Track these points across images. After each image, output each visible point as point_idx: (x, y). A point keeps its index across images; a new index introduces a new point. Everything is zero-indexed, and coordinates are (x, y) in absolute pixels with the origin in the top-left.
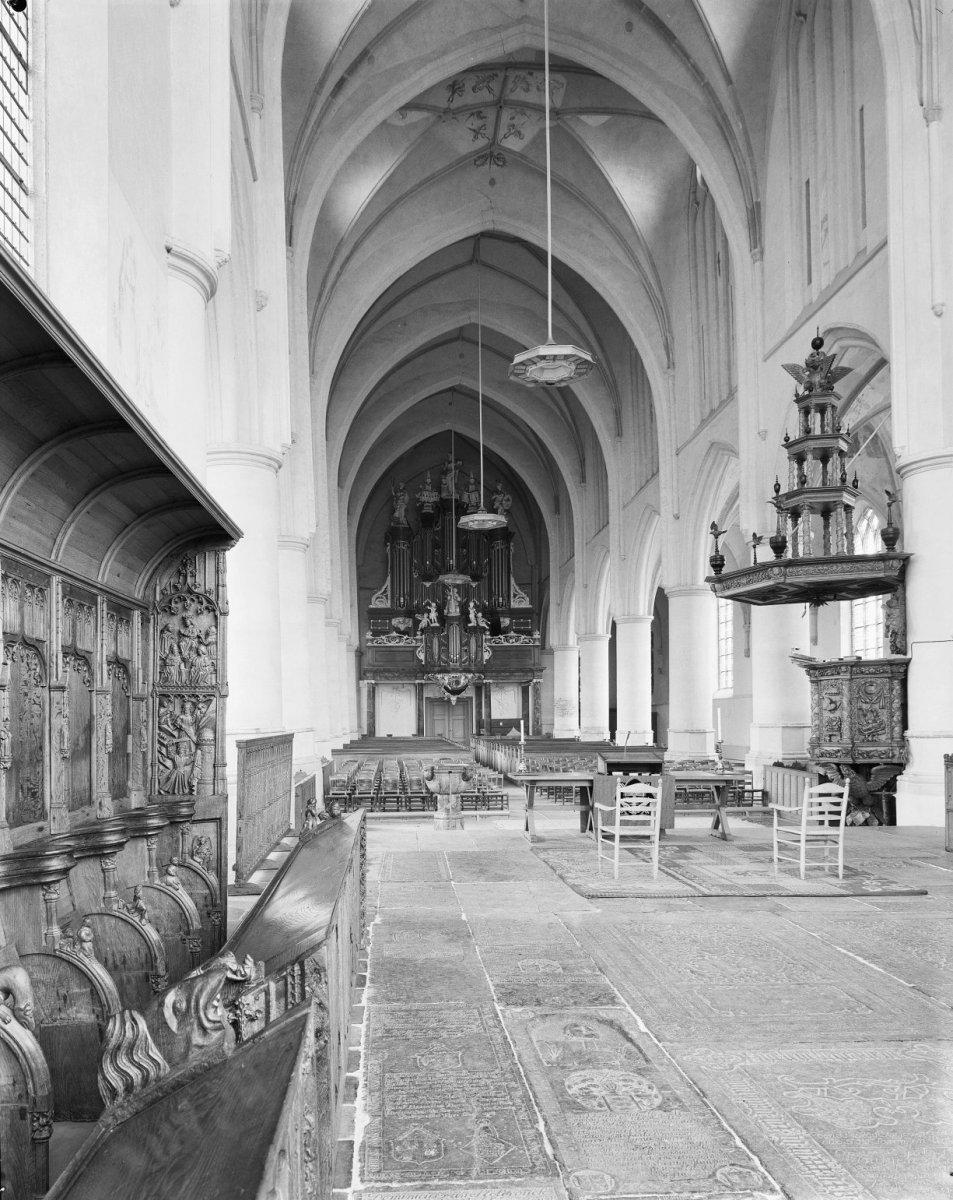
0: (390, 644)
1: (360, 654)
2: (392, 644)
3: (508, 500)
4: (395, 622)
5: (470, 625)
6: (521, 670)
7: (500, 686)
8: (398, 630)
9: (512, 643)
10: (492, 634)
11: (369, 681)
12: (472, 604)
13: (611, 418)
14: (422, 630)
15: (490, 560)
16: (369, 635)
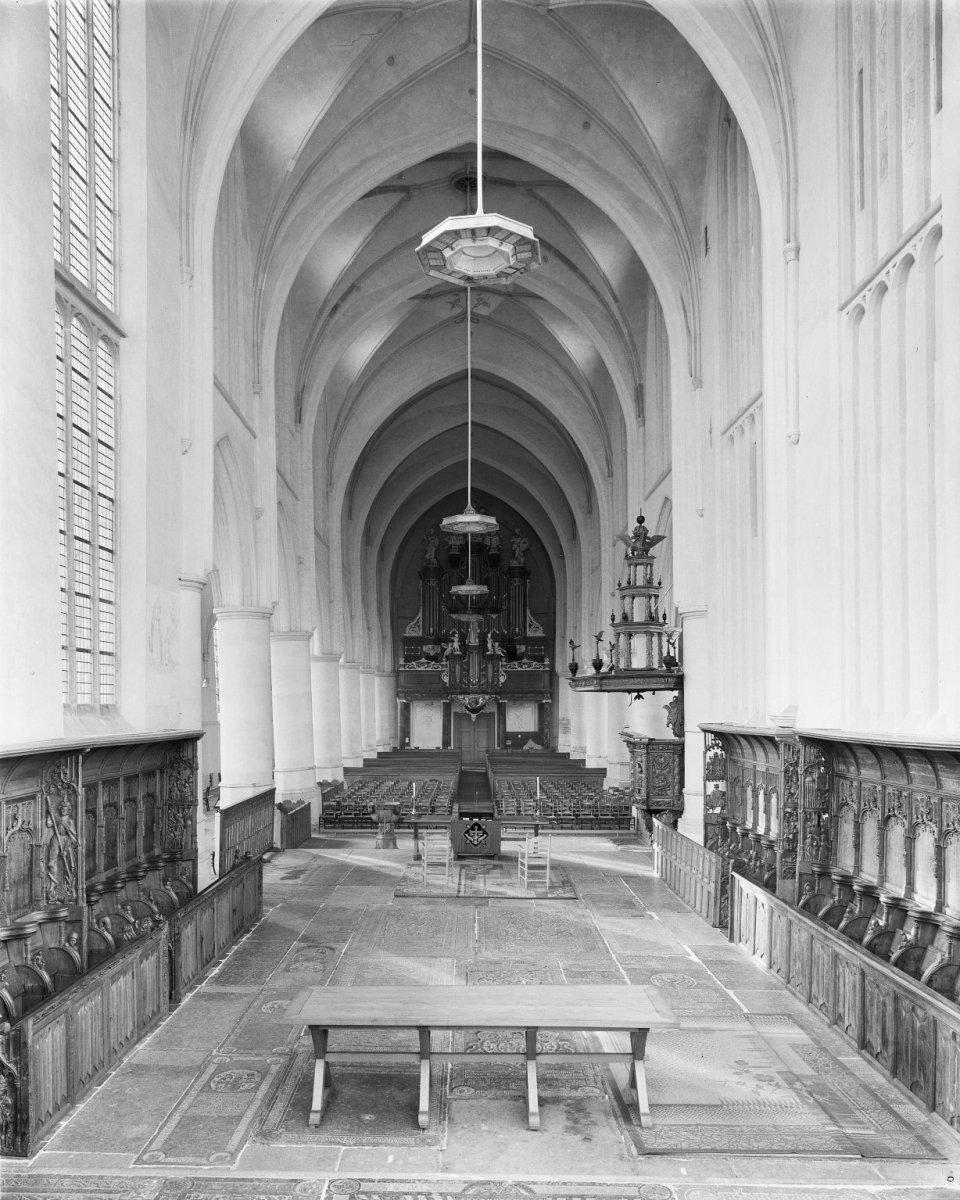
1: (396, 673)
2: (422, 668)
3: (525, 543)
4: (426, 648)
6: (533, 692)
8: (429, 657)
9: (525, 668)
12: (489, 635)
13: (584, 499)
16: (402, 661)
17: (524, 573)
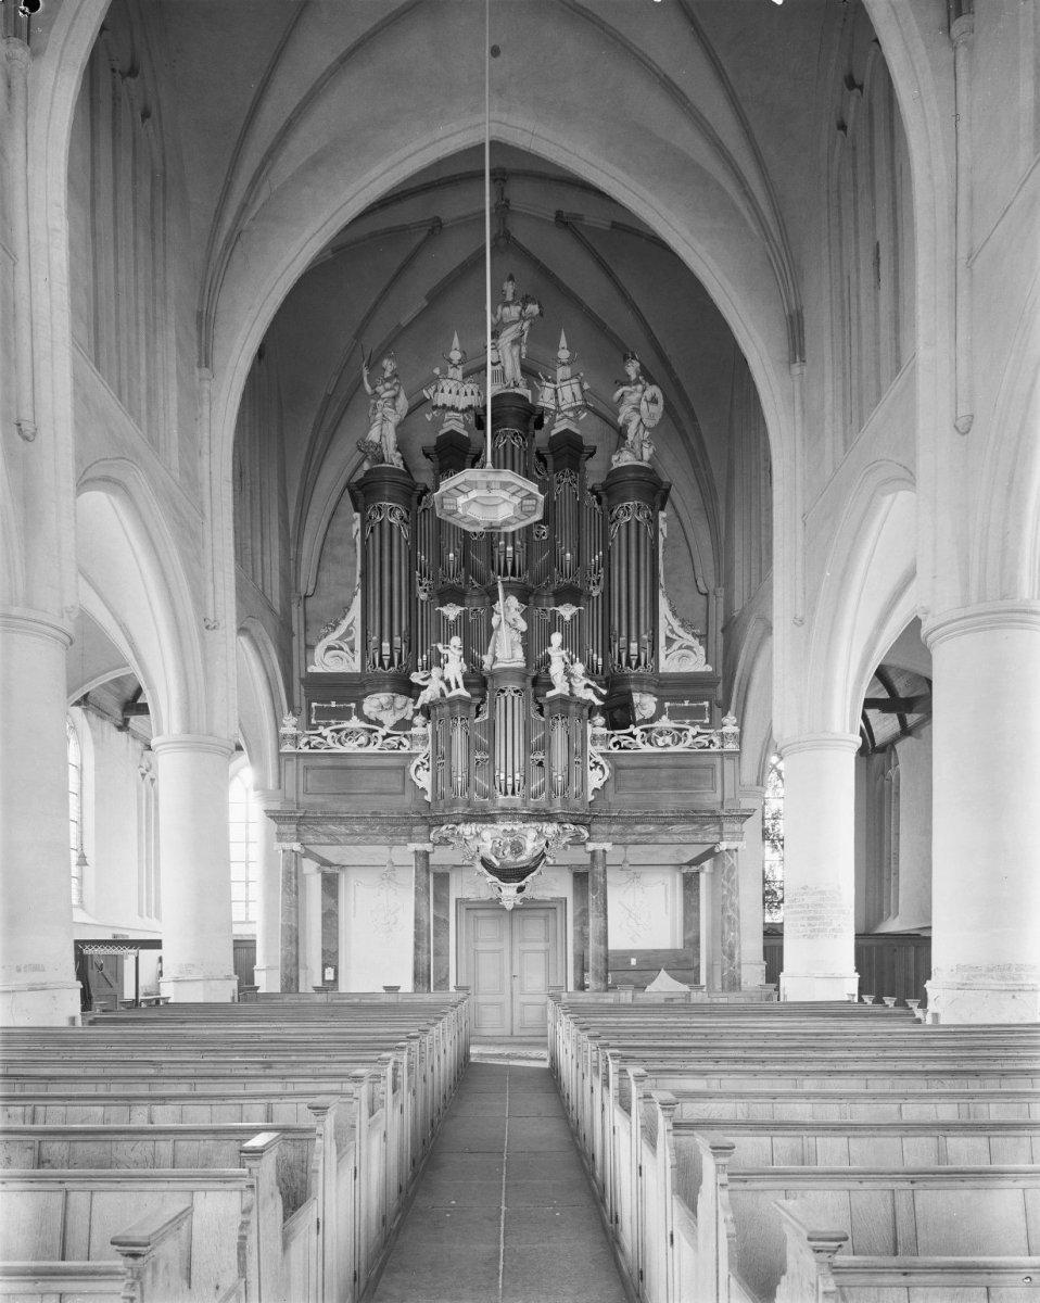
0: (342, 750)
2: (350, 747)
7: (635, 869)
10: (612, 724)
15: (608, 553)
17: (654, 491)
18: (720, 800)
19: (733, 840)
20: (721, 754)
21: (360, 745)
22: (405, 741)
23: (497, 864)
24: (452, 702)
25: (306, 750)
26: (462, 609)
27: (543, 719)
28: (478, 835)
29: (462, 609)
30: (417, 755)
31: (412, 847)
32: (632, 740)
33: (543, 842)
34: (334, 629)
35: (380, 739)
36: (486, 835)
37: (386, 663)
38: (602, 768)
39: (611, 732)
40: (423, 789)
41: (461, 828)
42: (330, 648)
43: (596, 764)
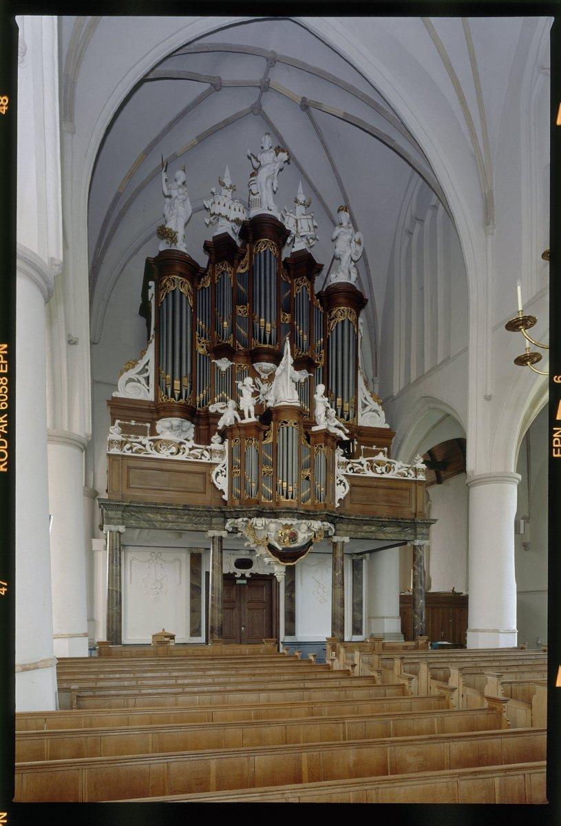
2: (164, 454)
5: (314, 429)
11: (113, 528)
14: (224, 434)
18: (414, 511)
19: (422, 539)
20: (416, 481)
21: (172, 454)
22: (205, 453)
23: (280, 549)
24: (247, 427)
25: (129, 453)
26: (231, 364)
27: (309, 446)
28: (266, 527)
29: (231, 364)
30: (217, 464)
31: (211, 533)
32: (361, 467)
33: (312, 534)
34: (133, 367)
35: (187, 451)
36: (273, 526)
37: (177, 396)
38: (344, 485)
39: (348, 460)
40: (222, 492)
41: (255, 520)
42: (131, 380)
43: (341, 481)
